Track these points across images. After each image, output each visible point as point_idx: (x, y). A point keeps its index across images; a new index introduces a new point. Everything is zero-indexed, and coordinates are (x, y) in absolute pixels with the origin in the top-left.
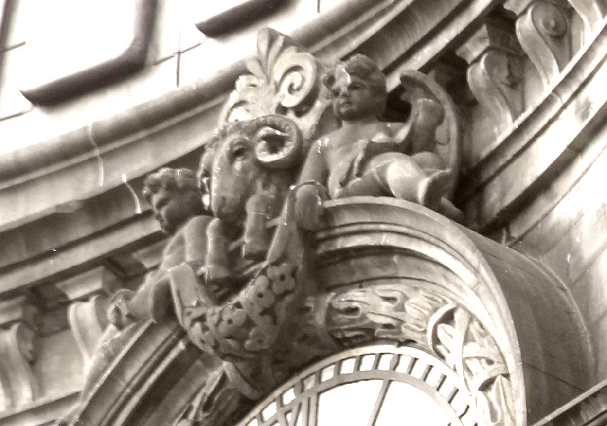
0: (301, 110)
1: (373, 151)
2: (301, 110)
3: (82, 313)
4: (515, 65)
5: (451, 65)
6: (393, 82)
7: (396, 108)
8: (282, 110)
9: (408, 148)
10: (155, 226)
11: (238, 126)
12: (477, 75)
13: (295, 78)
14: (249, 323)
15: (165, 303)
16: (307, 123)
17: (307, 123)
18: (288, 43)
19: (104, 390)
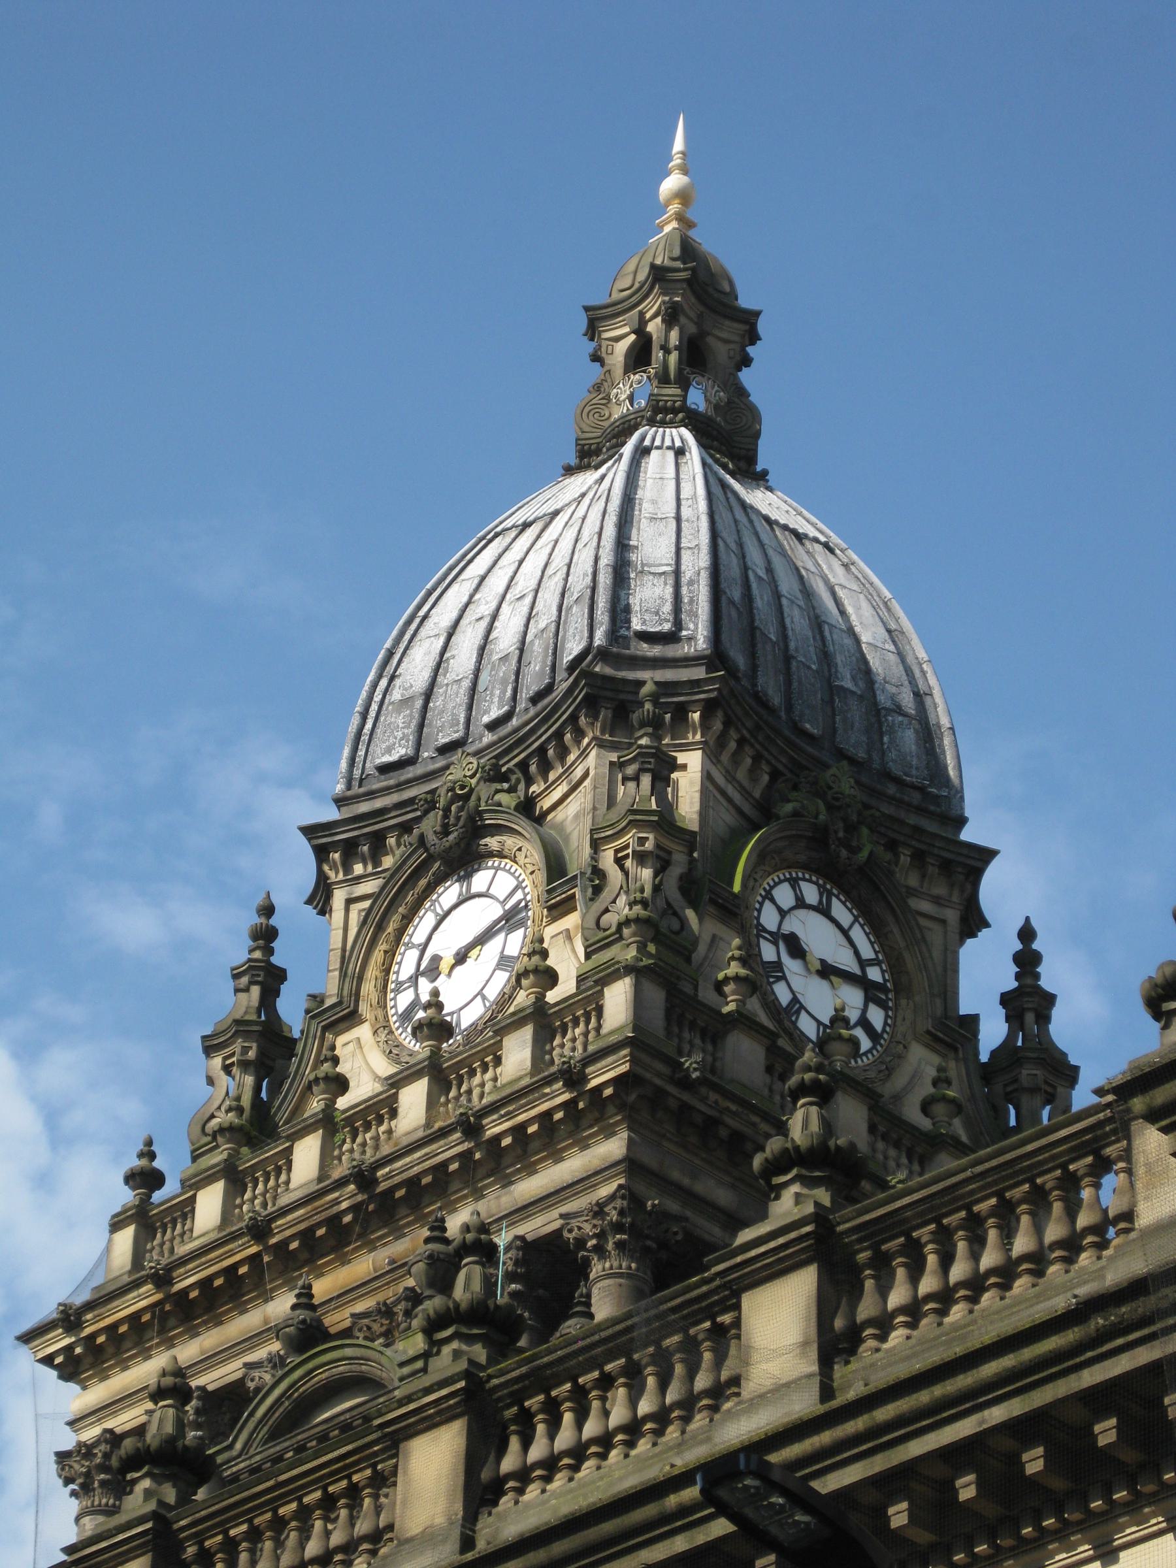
0: (472, 777)
1: (497, 791)
2: (472, 777)
3: (391, 841)
4: (546, 767)
5: (523, 766)
6: (504, 769)
7: (504, 778)
8: (465, 776)
9: (509, 791)
10: (419, 813)
11: (450, 781)
12: (533, 768)
13: (470, 766)
14: (451, 847)
15: (422, 838)
16: (474, 781)
17: (474, 781)
18: (468, 754)
19: (398, 868)
